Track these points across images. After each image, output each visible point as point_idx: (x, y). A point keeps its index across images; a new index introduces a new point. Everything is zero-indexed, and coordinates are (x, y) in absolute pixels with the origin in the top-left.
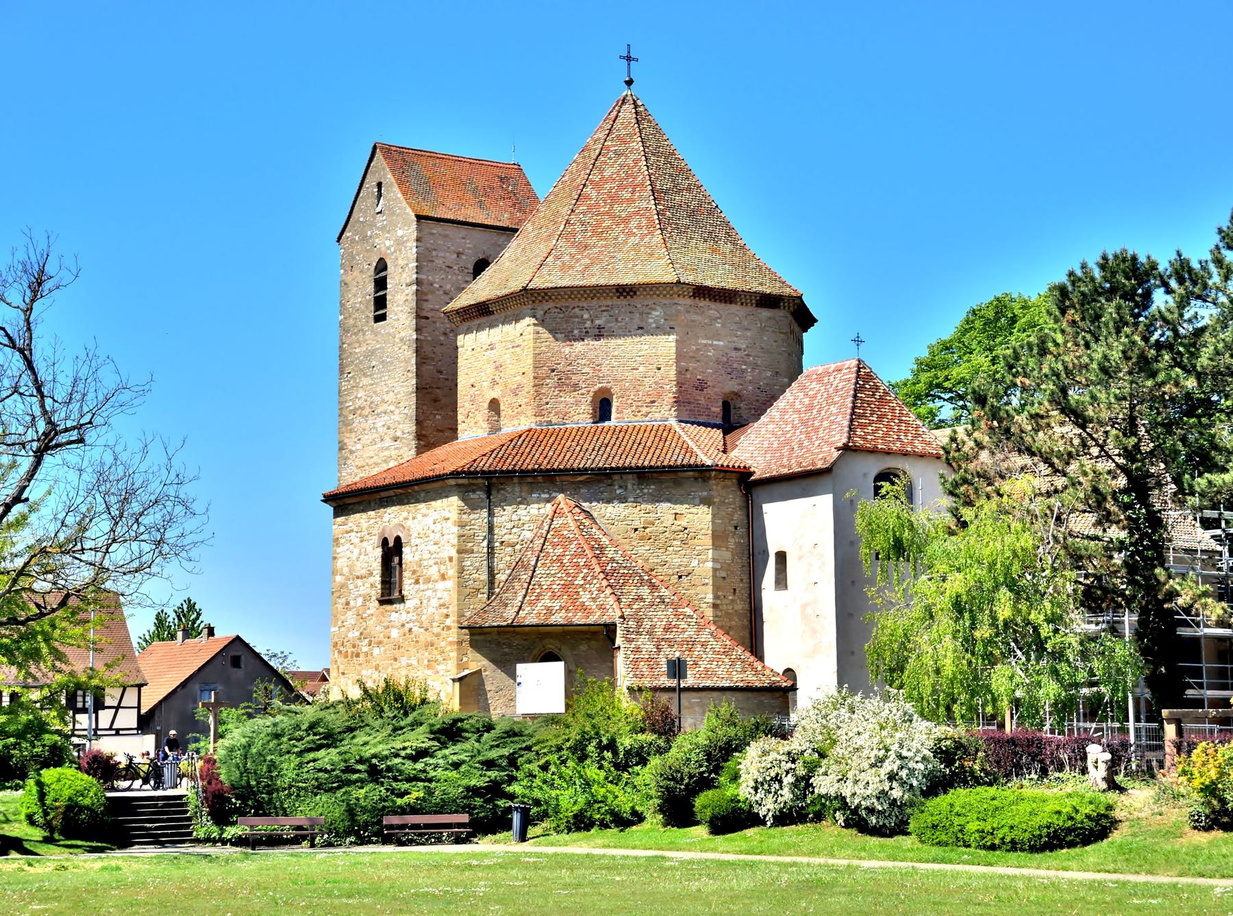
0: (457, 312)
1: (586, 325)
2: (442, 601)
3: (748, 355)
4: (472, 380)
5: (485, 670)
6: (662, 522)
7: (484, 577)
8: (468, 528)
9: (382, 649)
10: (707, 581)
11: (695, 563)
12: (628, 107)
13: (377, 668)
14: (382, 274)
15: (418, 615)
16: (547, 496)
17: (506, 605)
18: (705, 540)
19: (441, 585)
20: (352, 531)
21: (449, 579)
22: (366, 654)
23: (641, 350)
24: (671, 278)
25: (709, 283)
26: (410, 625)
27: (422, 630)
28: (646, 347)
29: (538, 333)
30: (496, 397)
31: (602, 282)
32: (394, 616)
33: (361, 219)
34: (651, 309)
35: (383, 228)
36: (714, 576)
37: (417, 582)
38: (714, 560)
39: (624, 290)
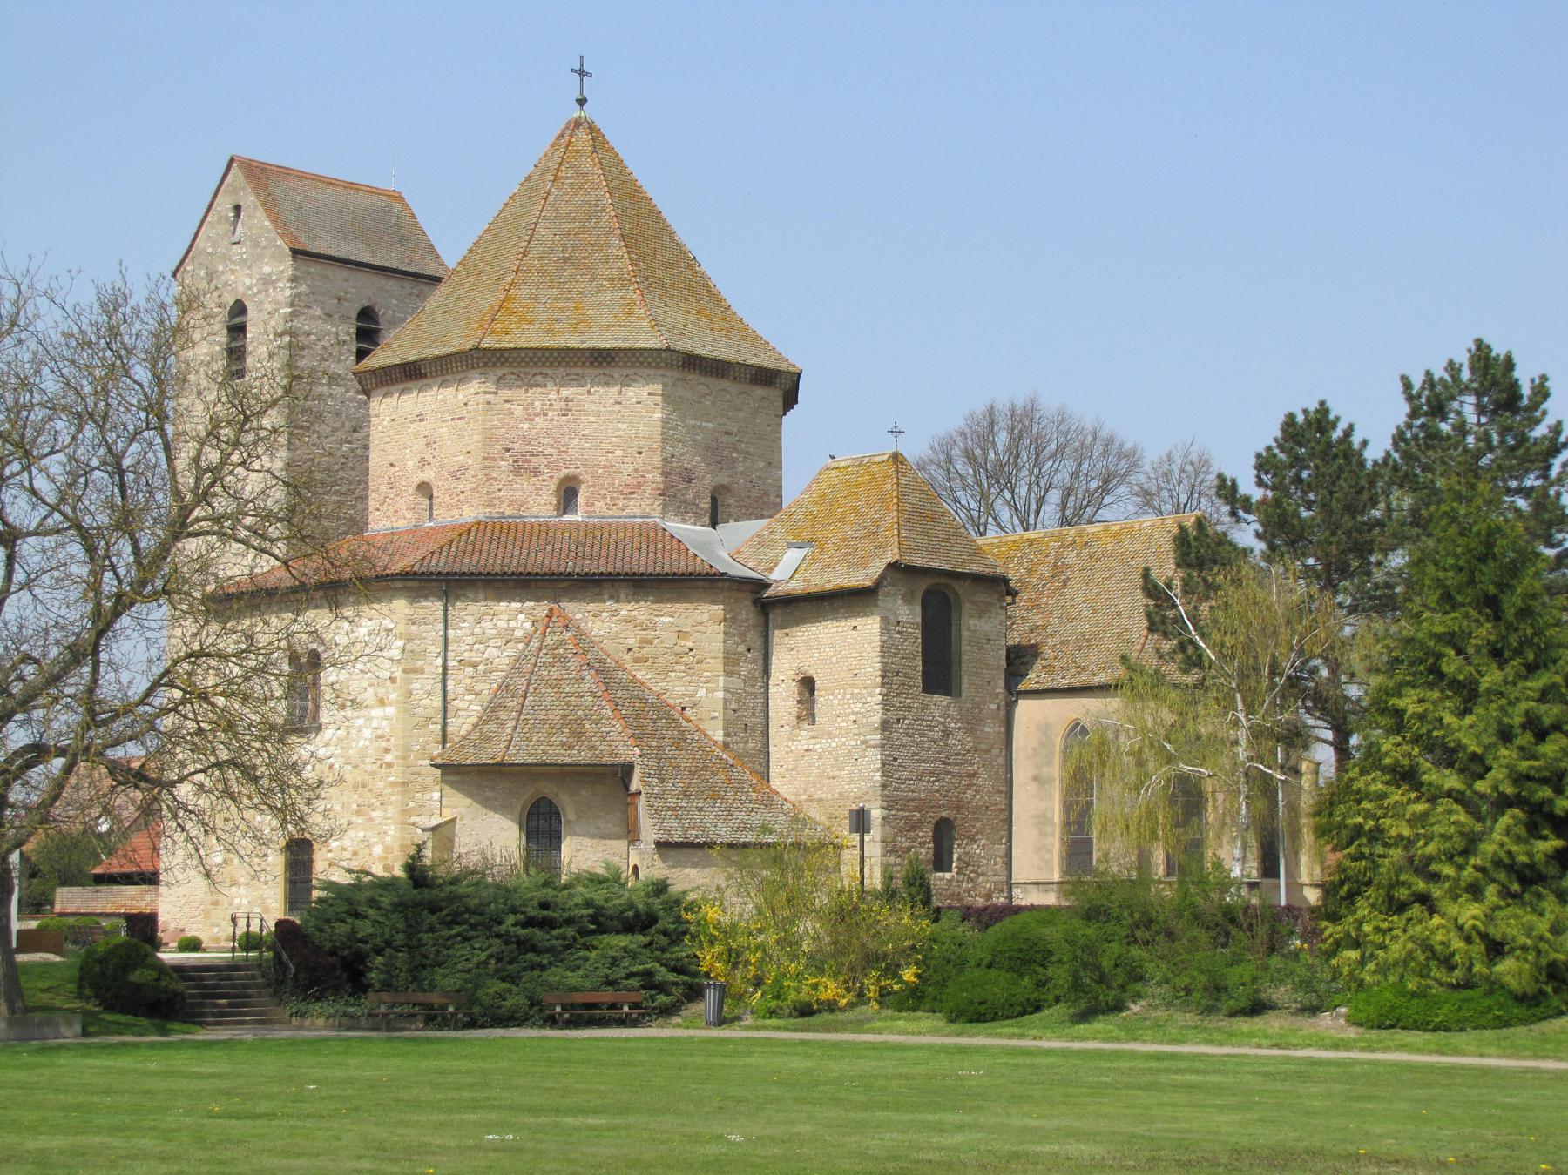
0: (374, 372)
1: (550, 397)
3: (739, 441)
4: (391, 458)
5: (462, 819)
6: (662, 642)
7: (437, 702)
8: (417, 642)
10: (716, 714)
11: (702, 693)
12: (582, 133)
14: (238, 320)
15: (342, 748)
16: (518, 605)
17: (489, 739)
18: (715, 665)
19: (377, 712)
23: (619, 430)
24: (655, 342)
25: (701, 352)
28: (625, 426)
29: (489, 403)
30: (426, 480)
31: (573, 343)
33: (210, 250)
34: (632, 380)
35: (243, 262)
36: (725, 708)
38: (726, 690)
39: (600, 355)
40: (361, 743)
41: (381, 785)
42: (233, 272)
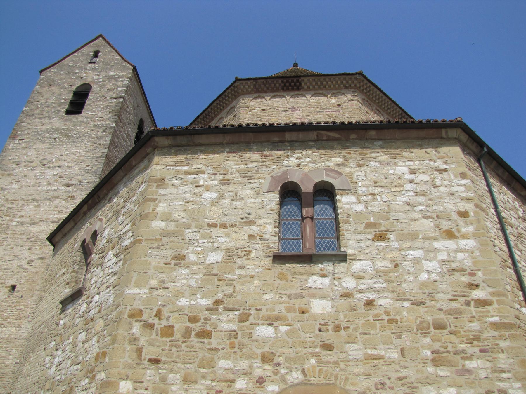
2: (454, 265)
9: (283, 329)
13: (266, 359)
20: (202, 172)
21: (465, 236)
22: (233, 335)
26: (371, 296)
27: (406, 304)
32: (315, 281)
37: (382, 237)
40: (424, 276)
41: (475, 326)
42: (85, 73)
